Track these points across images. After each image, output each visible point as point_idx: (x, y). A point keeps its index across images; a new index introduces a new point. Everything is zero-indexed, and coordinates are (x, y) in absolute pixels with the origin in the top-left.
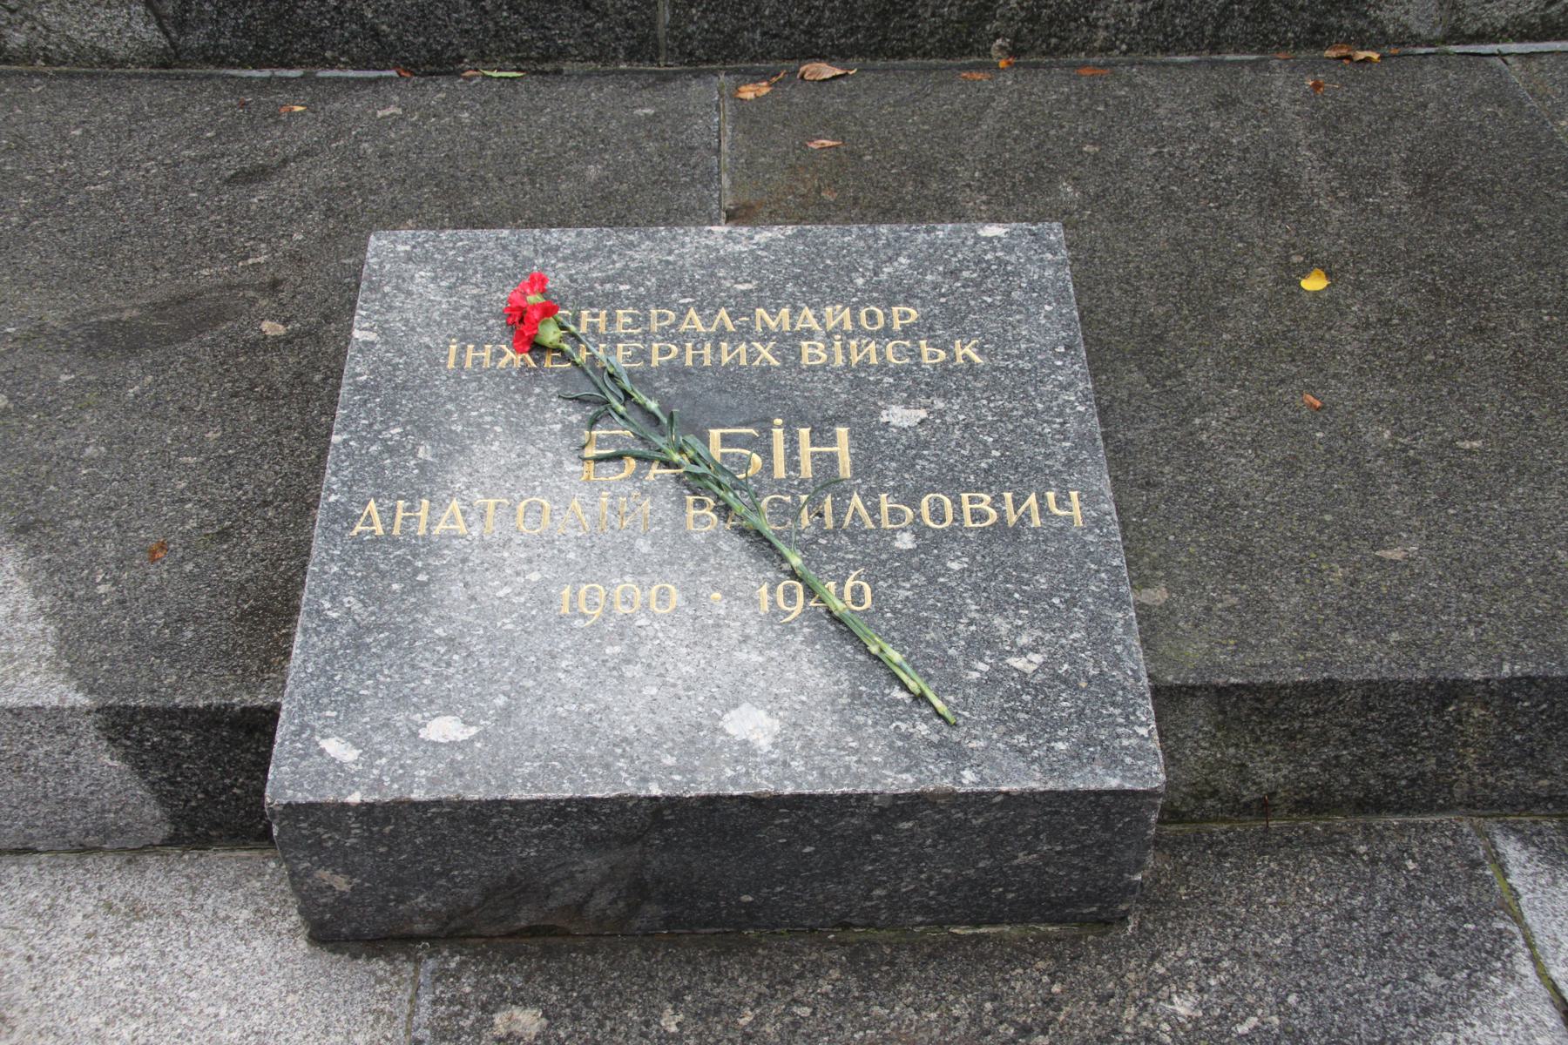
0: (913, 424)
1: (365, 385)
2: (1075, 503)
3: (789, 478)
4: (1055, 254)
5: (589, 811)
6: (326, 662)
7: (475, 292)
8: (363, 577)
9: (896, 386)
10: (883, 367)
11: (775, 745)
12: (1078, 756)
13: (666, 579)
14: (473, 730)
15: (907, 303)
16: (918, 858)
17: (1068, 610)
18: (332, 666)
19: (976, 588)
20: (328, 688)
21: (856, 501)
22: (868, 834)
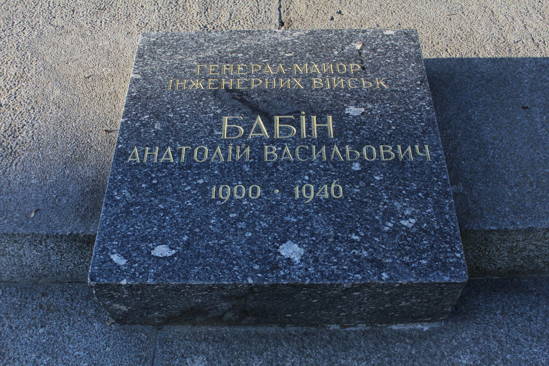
1: (135, 97)
2: (428, 151)
3: (307, 138)
4: (415, 42)
6: (114, 219)
7: (181, 57)
8: (131, 181)
9: (351, 98)
10: (346, 89)
11: (301, 260)
12: (431, 267)
13: (255, 183)
14: (174, 252)
18: (116, 221)
19: (387, 188)
20: (115, 231)
21: (336, 149)
22: (341, 296)
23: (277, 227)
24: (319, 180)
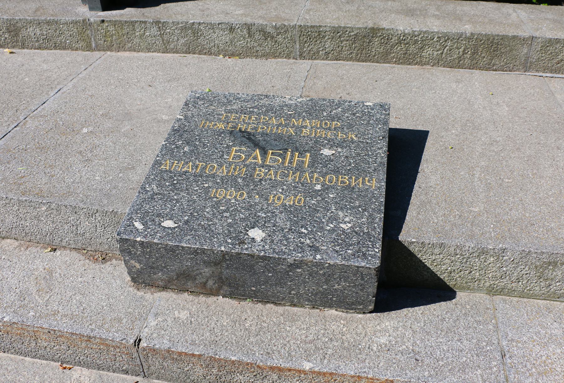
0: (330, 154)
5: (204, 253)
10: (325, 138)
14: (176, 225)
15: (338, 121)
16: (305, 282)
17: (363, 212)
19: (336, 203)
22: (288, 272)
23: (250, 218)
24: (289, 193)
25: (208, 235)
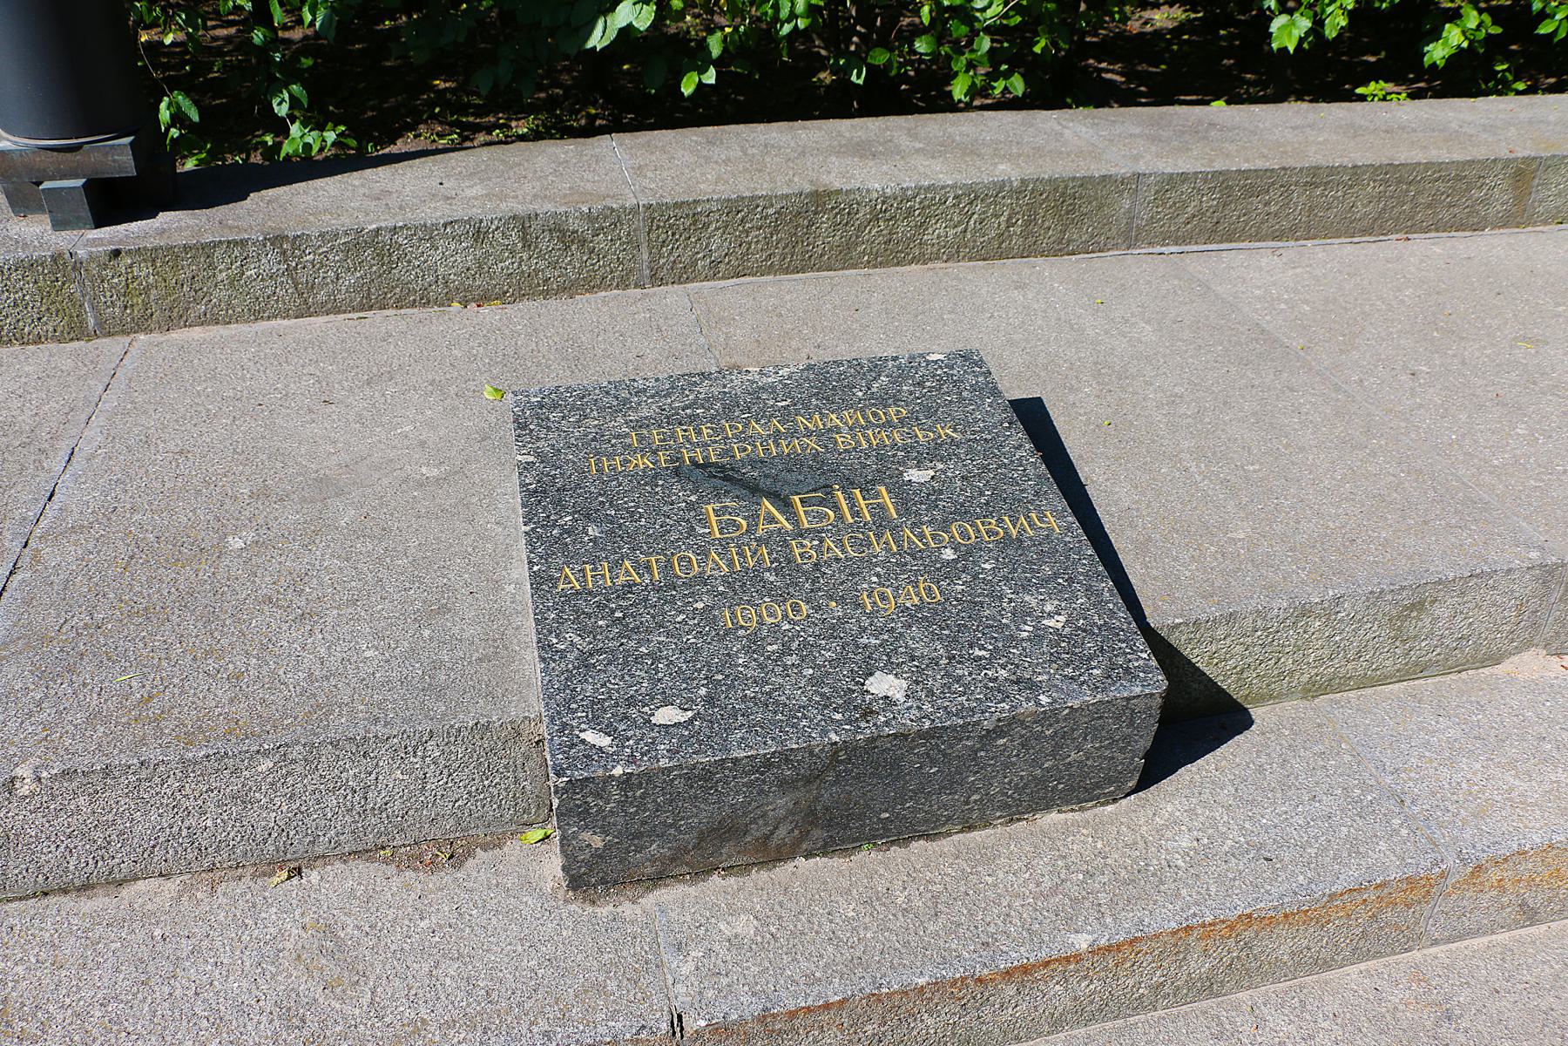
1: (535, 491)
5: (787, 760)
14: (690, 714)
19: (1006, 578)
25: (780, 716)
